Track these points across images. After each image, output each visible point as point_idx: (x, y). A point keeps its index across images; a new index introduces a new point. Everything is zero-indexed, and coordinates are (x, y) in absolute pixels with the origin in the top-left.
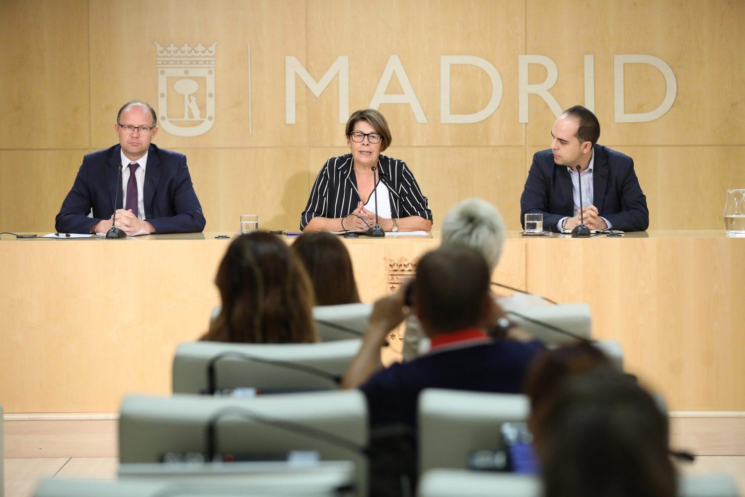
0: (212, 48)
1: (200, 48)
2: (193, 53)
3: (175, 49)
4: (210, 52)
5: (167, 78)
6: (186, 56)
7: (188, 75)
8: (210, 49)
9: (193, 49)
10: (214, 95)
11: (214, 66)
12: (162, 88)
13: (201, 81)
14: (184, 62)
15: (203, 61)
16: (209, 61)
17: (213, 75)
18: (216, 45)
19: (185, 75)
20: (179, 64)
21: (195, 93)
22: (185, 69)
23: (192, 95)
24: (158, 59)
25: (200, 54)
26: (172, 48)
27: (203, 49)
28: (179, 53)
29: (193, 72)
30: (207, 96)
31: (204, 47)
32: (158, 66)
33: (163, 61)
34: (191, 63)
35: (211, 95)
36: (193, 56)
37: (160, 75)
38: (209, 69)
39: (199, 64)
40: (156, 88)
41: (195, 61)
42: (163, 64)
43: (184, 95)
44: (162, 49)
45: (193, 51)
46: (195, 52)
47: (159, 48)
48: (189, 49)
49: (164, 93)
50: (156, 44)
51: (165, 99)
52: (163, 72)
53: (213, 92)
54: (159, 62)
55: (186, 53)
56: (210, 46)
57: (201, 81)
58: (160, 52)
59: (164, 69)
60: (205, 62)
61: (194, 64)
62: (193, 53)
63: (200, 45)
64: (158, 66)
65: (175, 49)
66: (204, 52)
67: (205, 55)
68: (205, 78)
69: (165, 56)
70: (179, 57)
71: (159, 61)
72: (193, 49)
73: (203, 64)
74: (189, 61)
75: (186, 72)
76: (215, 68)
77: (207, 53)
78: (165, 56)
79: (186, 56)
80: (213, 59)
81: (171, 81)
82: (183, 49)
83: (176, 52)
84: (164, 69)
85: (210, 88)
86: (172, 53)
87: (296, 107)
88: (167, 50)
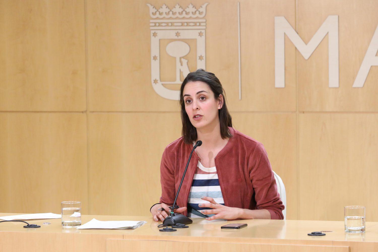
0: (203, 10)
1: (191, 9)
2: (184, 15)
3: (167, 10)
4: (200, 13)
5: (160, 40)
6: (177, 18)
7: (179, 38)
8: (201, 10)
9: (184, 10)
10: (204, 58)
11: (204, 27)
12: (155, 51)
13: (191, 43)
14: (175, 24)
15: (193, 23)
16: (200, 23)
17: (203, 37)
18: (208, 5)
19: (176, 38)
20: (171, 26)
21: (186, 56)
22: (176, 31)
23: (183, 57)
24: (151, 21)
25: (191, 15)
26: (164, 10)
27: (194, 10)
28: (171, 15)
29: (185, 34)
30: (198, 58)
31: (194, 8)
32: (152, 28)
33: (155, 23)
34: (182, 24)
35: (201, 58)
36: (184, 18)
37: (153, 38)
38: (199, 31)
39: (190, 26)
40: (149, 51)
41: (187, 23)
42: (155, 26)
43: (175, 58)
44: (154, 10)
45: (184, 13)
46: (187, 13)
47: (152, 10)
48: (181, 10)
49: (156, 56)
50: (149, 5)
51: (158, 61)
52: (155, 35)
53: (204, 55)
54: (151, 25)
55: (178, 15)
56: (202, 7)
57: (191, 43)
58: (153, 13)
59: (156, 31)
60: (195, 24)
61: (185, 26)
62: (184, 15)
63: (191, 6)
64: (152, 28)
65: (167, 10)
66: (194, 13)
67: (195, 16)
68: (196, 39)
69: (157, 18)
70: (170, 18)
71: (152, 23)
72: (184, 10)
73: (193, 26)
74: (180, 22)
75: (177, 34)
76: (205, 29)
77: (197, 14)
78: (157, 18)
79: (177, 18)
80: (204, 21)
81: (163, 44)
82: (174, 10)
83: (167, 14)
84: (156, 31)
85: (201, 51)
86: (164, 15)
87: (285, 69)
88: (159, 12)
